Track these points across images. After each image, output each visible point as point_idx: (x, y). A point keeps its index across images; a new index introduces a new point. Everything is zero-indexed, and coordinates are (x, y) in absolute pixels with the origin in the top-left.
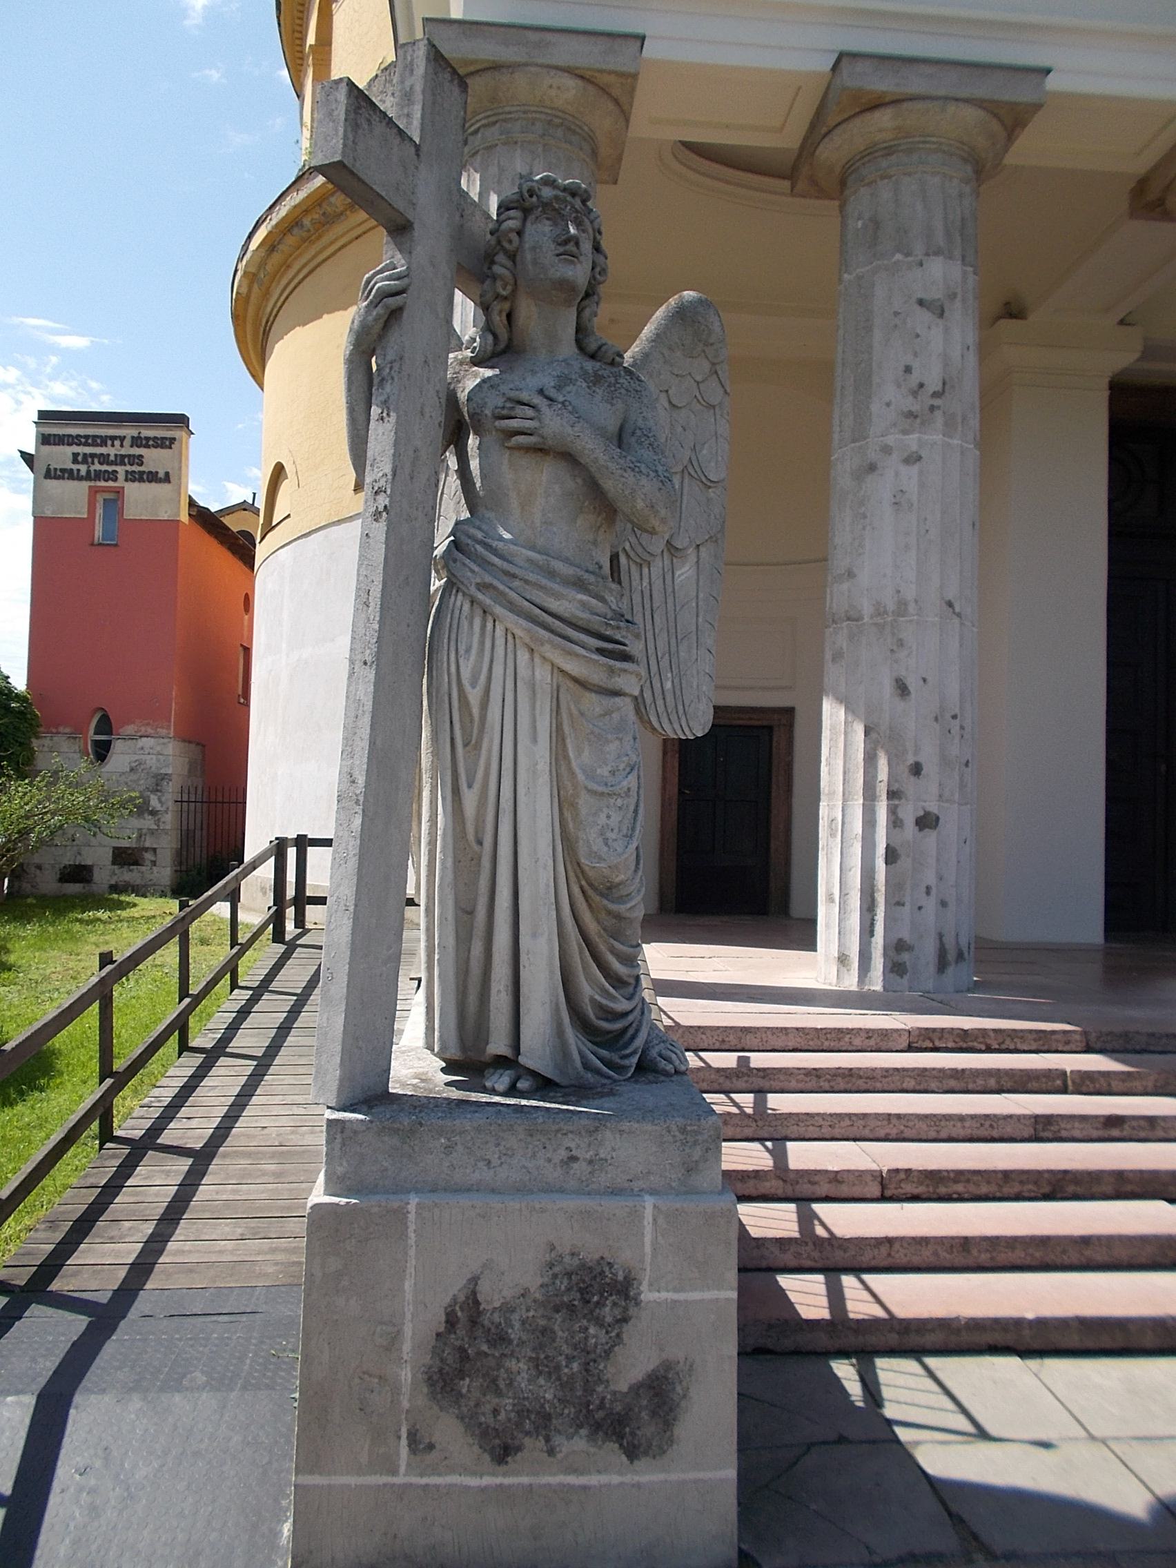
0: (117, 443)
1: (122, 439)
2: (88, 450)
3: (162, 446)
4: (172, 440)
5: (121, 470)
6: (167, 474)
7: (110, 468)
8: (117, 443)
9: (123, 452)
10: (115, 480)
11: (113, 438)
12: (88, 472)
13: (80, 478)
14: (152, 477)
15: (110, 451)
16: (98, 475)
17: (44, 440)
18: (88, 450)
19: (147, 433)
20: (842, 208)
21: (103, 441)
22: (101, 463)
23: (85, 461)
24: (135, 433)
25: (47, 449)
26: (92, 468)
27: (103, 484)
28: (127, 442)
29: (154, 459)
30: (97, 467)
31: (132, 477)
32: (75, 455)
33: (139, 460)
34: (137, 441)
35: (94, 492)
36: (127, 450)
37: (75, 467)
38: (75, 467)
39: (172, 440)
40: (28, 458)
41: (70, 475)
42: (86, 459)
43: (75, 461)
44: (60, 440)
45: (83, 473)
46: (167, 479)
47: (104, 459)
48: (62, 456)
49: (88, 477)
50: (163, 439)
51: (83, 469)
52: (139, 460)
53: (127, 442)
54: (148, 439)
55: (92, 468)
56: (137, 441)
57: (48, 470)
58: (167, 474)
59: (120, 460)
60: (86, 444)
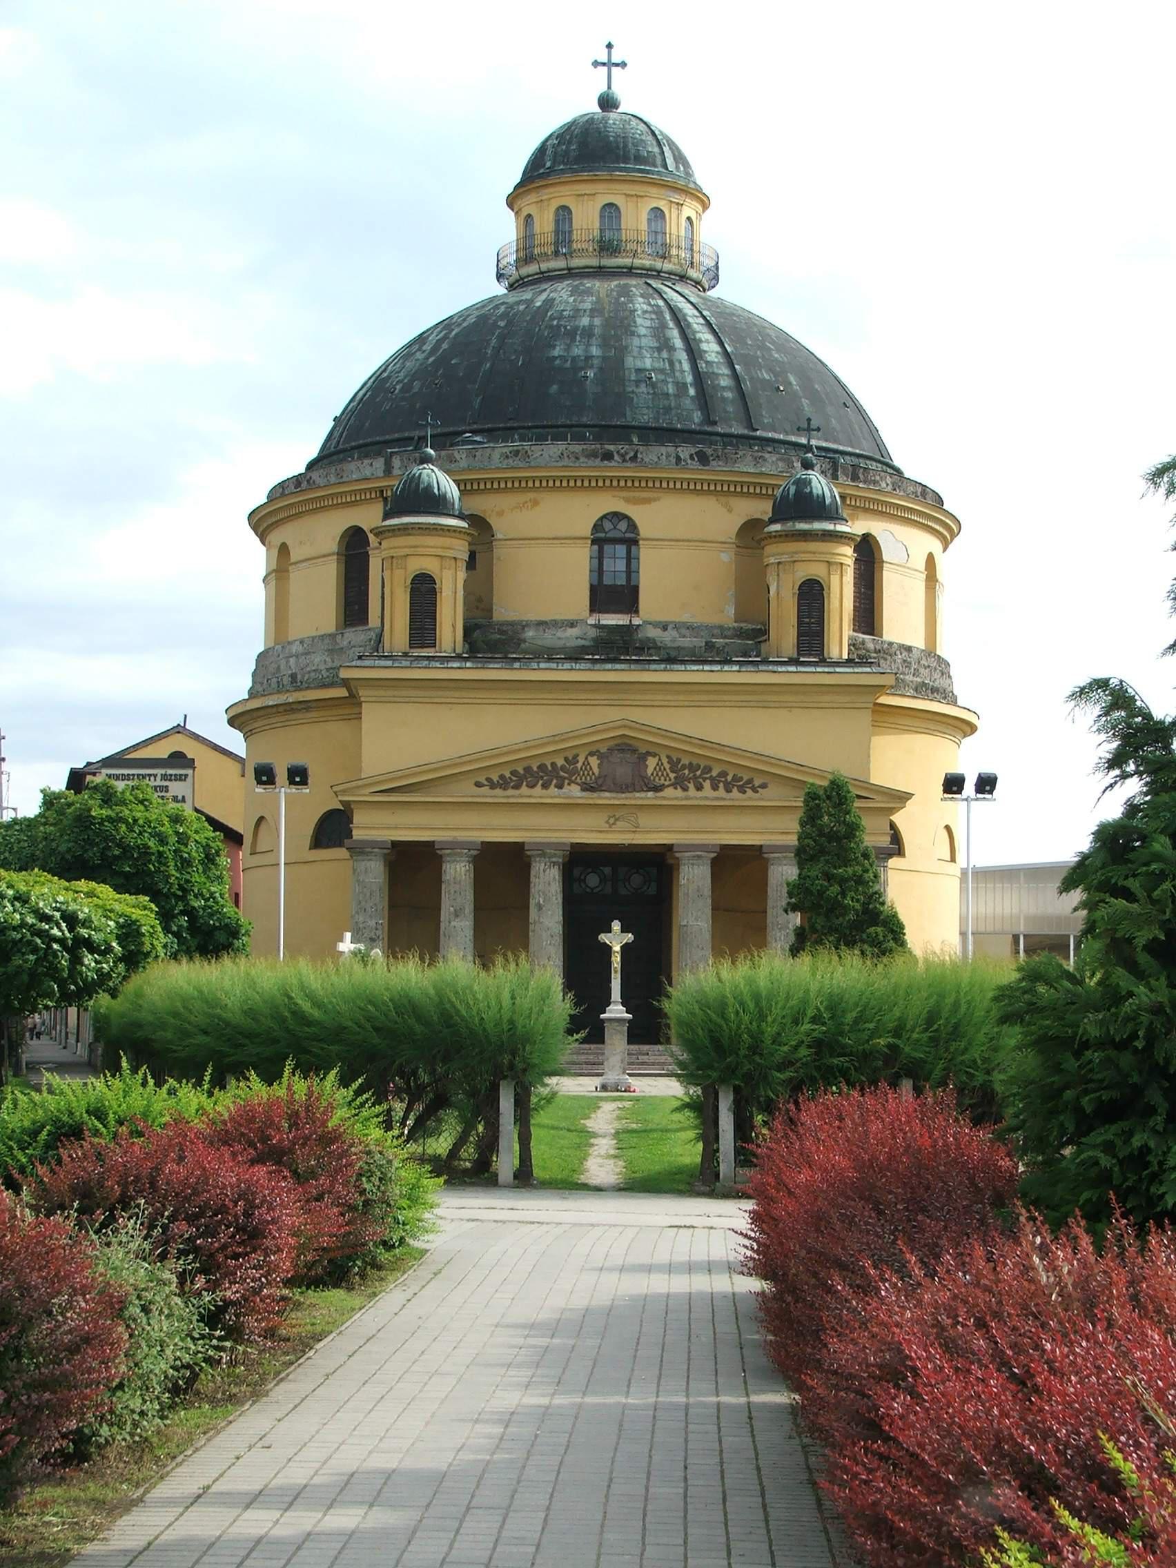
0: (152, 778)
1: (155, 776)
3: (180, 780)
4: (186, 776)
6: (183, 797)
8: (152, 778)
9: (157, 784)
11: (150, 775)
19: (170, 772)
20: (459, 657)
24: (163, 772)
28: (158, 778)
34: (164, 777)
36: (159, 783)
39: (186, 776)
50: (181, 775)
53: (158, 778)
54: (171, 775)
56: (164, 777)
58: (183, 797)
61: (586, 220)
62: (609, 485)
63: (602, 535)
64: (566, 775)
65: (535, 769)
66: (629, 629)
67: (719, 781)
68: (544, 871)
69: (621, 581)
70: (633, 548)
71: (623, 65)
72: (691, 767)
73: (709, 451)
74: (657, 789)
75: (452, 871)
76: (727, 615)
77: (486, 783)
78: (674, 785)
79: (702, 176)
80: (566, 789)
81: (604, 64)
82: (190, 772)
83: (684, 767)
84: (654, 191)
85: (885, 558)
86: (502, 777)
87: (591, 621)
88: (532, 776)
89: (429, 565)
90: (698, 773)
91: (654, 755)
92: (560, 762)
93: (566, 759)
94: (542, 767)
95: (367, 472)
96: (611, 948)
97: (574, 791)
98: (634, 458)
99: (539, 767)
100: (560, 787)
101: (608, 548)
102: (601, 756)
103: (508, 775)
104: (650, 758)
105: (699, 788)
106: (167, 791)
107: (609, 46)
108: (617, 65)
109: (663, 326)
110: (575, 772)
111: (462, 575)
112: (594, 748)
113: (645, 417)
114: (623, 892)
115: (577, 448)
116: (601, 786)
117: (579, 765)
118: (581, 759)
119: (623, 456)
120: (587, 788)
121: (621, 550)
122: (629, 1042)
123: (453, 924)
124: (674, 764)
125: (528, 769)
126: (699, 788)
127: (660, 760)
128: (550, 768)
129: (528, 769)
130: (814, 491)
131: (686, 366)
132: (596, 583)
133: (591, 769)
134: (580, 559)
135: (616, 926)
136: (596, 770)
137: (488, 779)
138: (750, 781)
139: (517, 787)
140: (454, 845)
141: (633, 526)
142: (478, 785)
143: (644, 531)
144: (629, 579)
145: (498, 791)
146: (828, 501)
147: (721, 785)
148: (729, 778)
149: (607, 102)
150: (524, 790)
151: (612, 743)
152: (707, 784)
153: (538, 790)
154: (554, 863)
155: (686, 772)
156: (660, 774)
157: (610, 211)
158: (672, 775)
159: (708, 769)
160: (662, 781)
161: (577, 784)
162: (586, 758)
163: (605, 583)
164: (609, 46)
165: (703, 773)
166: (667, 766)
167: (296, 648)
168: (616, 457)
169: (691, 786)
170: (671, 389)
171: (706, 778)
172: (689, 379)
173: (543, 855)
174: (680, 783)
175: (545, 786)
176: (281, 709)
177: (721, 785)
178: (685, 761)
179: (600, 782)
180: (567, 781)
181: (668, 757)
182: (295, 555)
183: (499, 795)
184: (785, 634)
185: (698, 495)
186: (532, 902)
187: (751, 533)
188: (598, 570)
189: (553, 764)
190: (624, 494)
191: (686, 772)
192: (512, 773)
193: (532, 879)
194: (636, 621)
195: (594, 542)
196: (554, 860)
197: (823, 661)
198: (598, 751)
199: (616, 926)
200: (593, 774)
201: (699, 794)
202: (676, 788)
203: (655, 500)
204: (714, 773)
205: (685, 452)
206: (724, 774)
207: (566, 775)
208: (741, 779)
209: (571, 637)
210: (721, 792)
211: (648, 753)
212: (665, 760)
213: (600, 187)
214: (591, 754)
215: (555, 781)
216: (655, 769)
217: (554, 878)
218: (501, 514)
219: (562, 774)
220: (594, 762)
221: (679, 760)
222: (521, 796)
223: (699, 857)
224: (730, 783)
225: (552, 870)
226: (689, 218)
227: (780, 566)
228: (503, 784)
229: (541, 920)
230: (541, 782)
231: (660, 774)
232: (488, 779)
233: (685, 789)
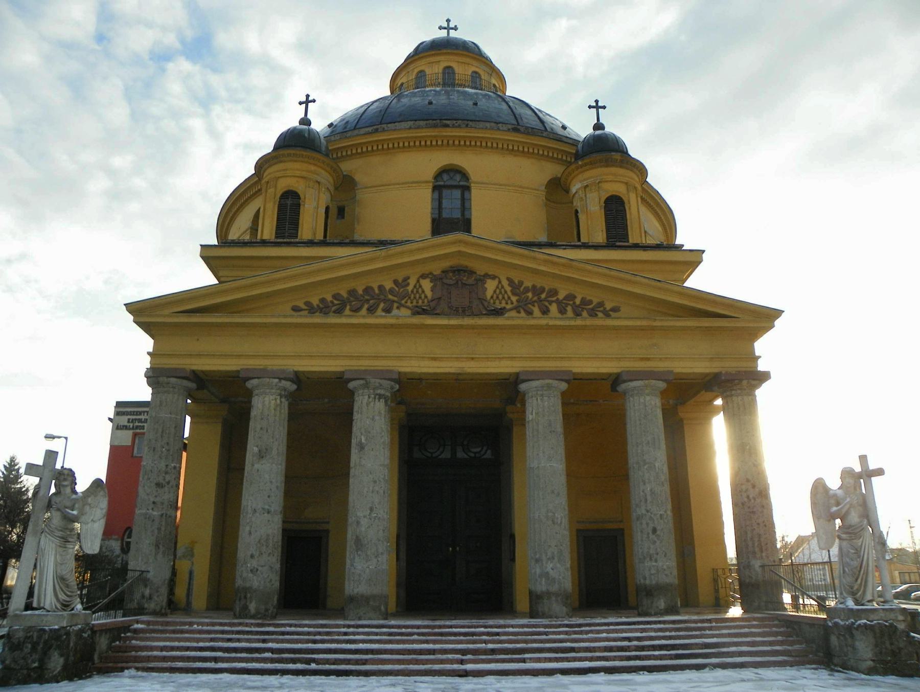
0: (146, 414)
2: (134, 417)
7: (142, 424)
8: (146, 414)
10: (144, 429)
11: (144, 412)
12: (133, 426)
13: (130, 429)
15: (142, 417)
16: (137, 427)
17: (117, 414)
18: (134, 417)
21: (140, 413)
22: (138, 422)
23: (132, 422)
25: (118, 417)
26: (135, 425)
27: (138, 431)
30: (137, 424)
32: (129, 419)
35: (135, 435)
37: (128, 424)
38: (128, 424)
40: (110, 419)
42: (133, 421)
43: (129, 422)
44: (123, 414)
45: (131, 427)
47: (140, 421)
48: (124, 420)
49: (133, 428)
51: (131, 425)
55: (135, 425)
57: (118, 426)
60: (134, 415)
63: (442, 183)
64: (395, 299)
65: (360, 292)
67: (567, 305)
68: (368, 404)
69: (457, 215)
70: (466, 194)
72: (537, 291)
74: (499, 312)
75: (260, 406)
77: (304, 307)
80: (395, 312)
81: (445, 28)
83: (527, 290)
84: (475, 63)
86: (323, 300)
88: (357, 299)
89: (299, 187)
90: (543, 296)
91: (494, 277)
92: (388, 285)
93: (396, 282)
94: (368, 290)
97: (402, 315)
101: (445, 192)
102: (434, 279)
103: (329, 298)
105: (545, 312)
108: (452, 29)
110: (406, 295)
114: (460, 454)
116: (434, 309)
117: (410, 288)
118: (412, 282)
120: (419, 311)
121: (457, 193)
123: (256, 466)
126: (545, 312)
127: (500, 282)
128: (377, 291)
132: (437, 216)
133: (423, 292)
136: (429, 294)
137: (307, 303)
138: (601, 304)
139: (339, 312)
140: (263, 373)
141: (464, 175)
142: (296, 309)
143: (473, 177)
144: (463, 214)
147: (569, 309)
148: (578, 301)
151: (446, 264)
152: (554, 308)
154: (380, 396)
156: (500, 297)
158: (514, 299)
160: (503, 305)
161: (408, 308)
162: (418, 281)
163: (444, 216)
165: (547, 297)
166: (508, 289)
169: (536, 311)
171: (553, 301)
173: (366, 386)
174: (523, 307)
175: (371, 310)
177: (569, 309)
178: (528, 284)
179: (433, 304)
180: (395, 305)
181: (508, 279)
183: (318, 319)
185: (515, 156)
188: (438, 206)
189: (381, 287)
191: (530, 295)
195: (435, 188)
196: (379, 391)
198: (431, 273)
200: (426, 297)
202: (519, 312)
204: (561, 296)
207: (395, 299)
208: (590, 302)
211: (487, 276)
212: (505, 283)
214: (423, 276)
215: (382, 305)
216: (495, 292)
217: (380, 413)
219: (390, 297)
220: (427, 285)
221: (521, 283)
223: (549, 387)
224: (578, 306)
225: (377, 403)
227: (587, 189)
228: (324, 308)
229: (363, 462)
230: (366, 306)
231: (500, 297)
233: (529, 313)
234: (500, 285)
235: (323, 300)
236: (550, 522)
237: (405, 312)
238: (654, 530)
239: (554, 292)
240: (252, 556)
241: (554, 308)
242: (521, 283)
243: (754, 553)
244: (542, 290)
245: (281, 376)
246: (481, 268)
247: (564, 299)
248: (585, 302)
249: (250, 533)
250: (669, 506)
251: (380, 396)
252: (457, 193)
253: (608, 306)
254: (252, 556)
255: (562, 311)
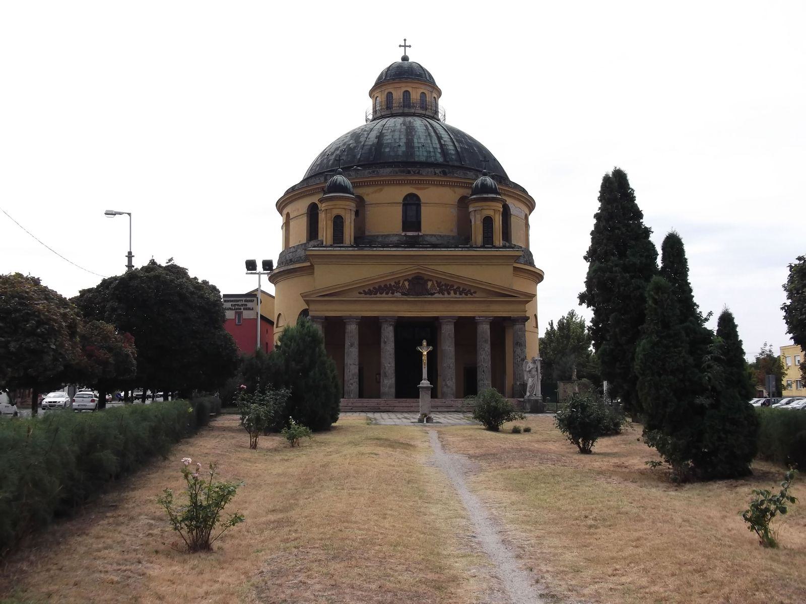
1: (242, 300)
3: (251, 302)
4: (254, 300)
5: (242, 308)
6: (253, 308)
11: (240, 300)
14: (249, 309)
15: (239, 303)
19: (248, 299)
20: (352, 246)
21: (238, 301)
28: (243, 301)
29: (250, 305)
30: (237, 307)
31: (244, 309)
33: (246, 305)
34: (246, 301)
35: (236, 313)
36: (243, 303)
39: (254, 300)
41: (231, 309)
44: (228, 301)
46: (253, 309)
47: (238, 305)
52: (246, 305)
53: (243, 301)
56: (246, 301)
58: (253, 308)
59: (242, 305)
61: (398, 95)
62: (410, 183)
65: (383, 286)
66: (418, 236)
68: (387, 327)
71: (410, 46)
72: (446, 285)
73: (447, 171)
74: (432, 294)
76: (454, 233)
78: (439, 293)
79: (439, 83)
80: (395, 294)
81: (403, 46)
82: (255, 299)
84: (423, 87)
85: (512, 213)
86: (369, 290)
87: (403, 234)
89: (341, 213)
90: (449, 287)
91: (431, 280)
92: (393, 284)
93: (395, 283)
94: (385, 286)
95: (318, 182)
96: (422, 353)
98: (418, 173)
99: (384, 286)
100: (393, 293)
103: (372, 289)
104: (429, 282)
105: (449, 294)
106: (246, 306)
107: (405, 40)
108: (408, 46)
109: (427, 129)
110: (399, 287)
111: (353, 217)
112: (407, 278)
113: (423, 159)
115: (397, 169)
119: (414, 172)
120: (403, 294)
121: (414, 207)
122: (431, 398)
124: (439, 284)
125: (380, 287)
126: (449, 294)
129: (380, 287)
130: (488, 183)
131: (437, 142)
134: (397, 213)
135: (425, 343)
136: (407, 287)
139: (376, 294)
140: (350, 317)
142: (360, 293)
143: (423, 200)
145: (368, 296)
146: (494, 187)
147: (458, 293)
148: (461, 290)
149: (405, 58)
150: (378, 295)
151: (413, 276)
152: (452, 292)
153: (384, 295)
155: (444, 287)
157: (407, 93)
158: (438, 289)
159: (452, 286)
164: (405, 40)
166: (436, 285)
167: (292, 250)
168: (412, 172)
169: (446, 293)
170: (432, 150)
172: (438, 146)
173: (386, 321)
174: (441, 292)
175: (387, 293)
176: (286, 272)
177: (458, 293)
181: (436, 281)
182: (291, 217)
184: (478, 236)
185: (443, 187)
186: (382, 340)
187: (463, 202)
189: (390, 285)
190: (416, 186)
191: (444, 287)
192: (373, 288)
193: (382, 331)
194: (420, 234)
197: (495, 247)
199: (425, 343)
201: (449, 296)
203: (427, 188)
205: (438, 171)
206: (459, 288)
209: (395, 239)
210: (458, 295)
212: (435, 282)
213: (403, 85)
214: (405, 280)
215: (391, 291)
218: (368, 195)
219: (394, 288)
220: (406, 284)
221: (441, 282)
222: (377, 297)
223: (449, 321)
226: (434, 98)
228: (370, 292)
232: (364, 291)
233: (443, 294)
234: (433, 284)
235: (369, 290)
236: (448, 368)
237: (398, 295)
238: (483, 371)
239: (452, 286)
240: (351, 379)
241: (452, 292)
242: (441, 282)
243: (518, 380)
244: (449, 285)
245: (356, 318)
246: (426, 278)
247: (456, 288)
248: (464, 290)
249: (349, 372)
250: (490, 363)
251: (391, 325)
252: (414, 207)
253: (472, 291)
254: (351, 379)
255: (455, 293)
